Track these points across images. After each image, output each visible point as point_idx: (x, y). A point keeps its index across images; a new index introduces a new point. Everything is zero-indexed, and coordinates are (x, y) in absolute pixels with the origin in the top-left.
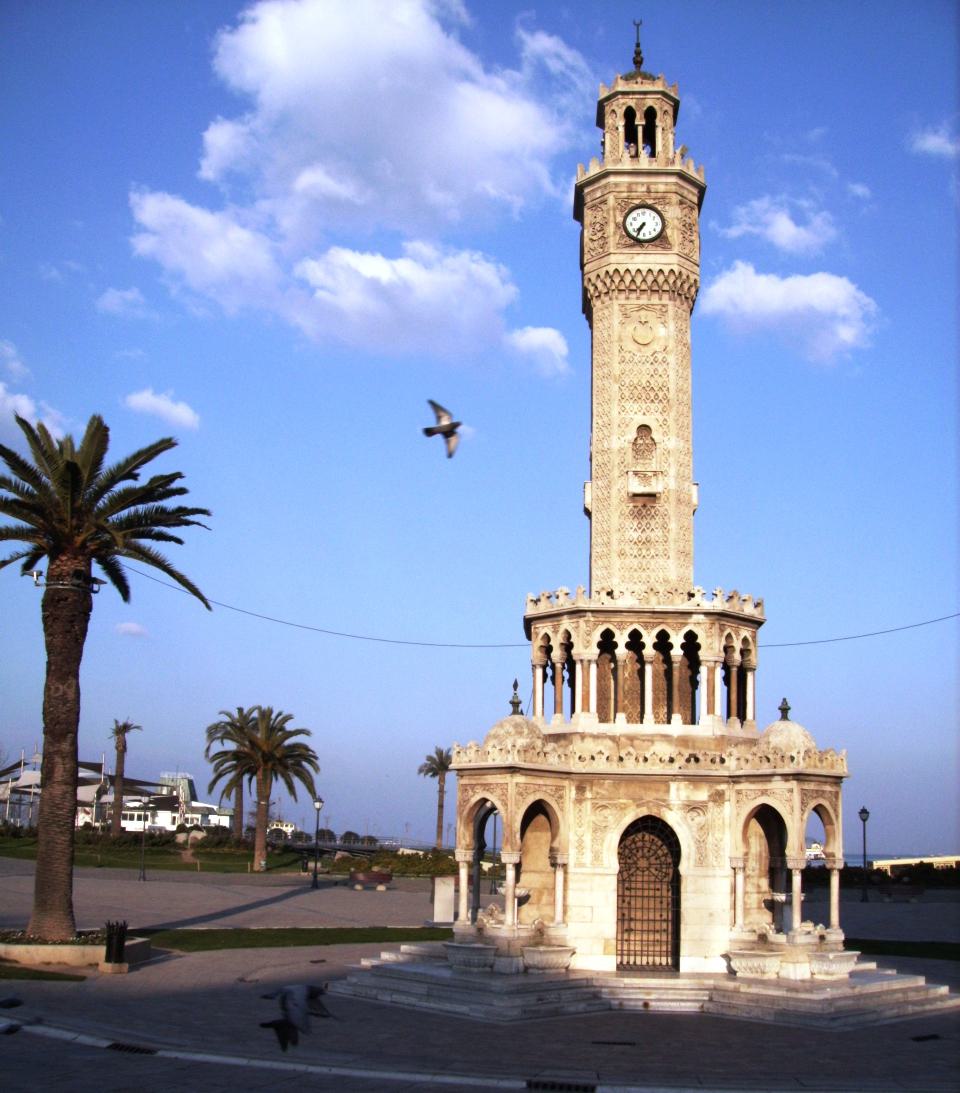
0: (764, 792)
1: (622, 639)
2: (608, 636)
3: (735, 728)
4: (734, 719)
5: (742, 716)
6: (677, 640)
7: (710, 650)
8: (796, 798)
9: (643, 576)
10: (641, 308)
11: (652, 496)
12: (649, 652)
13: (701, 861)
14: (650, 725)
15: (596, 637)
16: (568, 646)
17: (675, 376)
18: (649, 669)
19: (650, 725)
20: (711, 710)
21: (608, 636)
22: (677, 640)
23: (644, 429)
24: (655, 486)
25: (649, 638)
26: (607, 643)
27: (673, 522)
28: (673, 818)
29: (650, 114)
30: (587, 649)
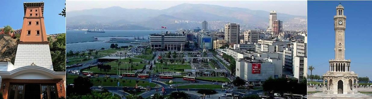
2: (337, 63)
5: (349, 71)
6: (343, 64)
7: (346, 64)
9: (340, 58)
11: (341, 50)
12: (340, 65)
13: (345, 84)
15: (336, 64)
16: (333, 64)
17: (343, 38)
21: (337, 63)
22: (343, 64)
23: (340, 43)
24: (341, 49)
26: (337, 64)
27: (343, 52)
28: (342, 80)
29: (341, 10)
30: (335, 65)
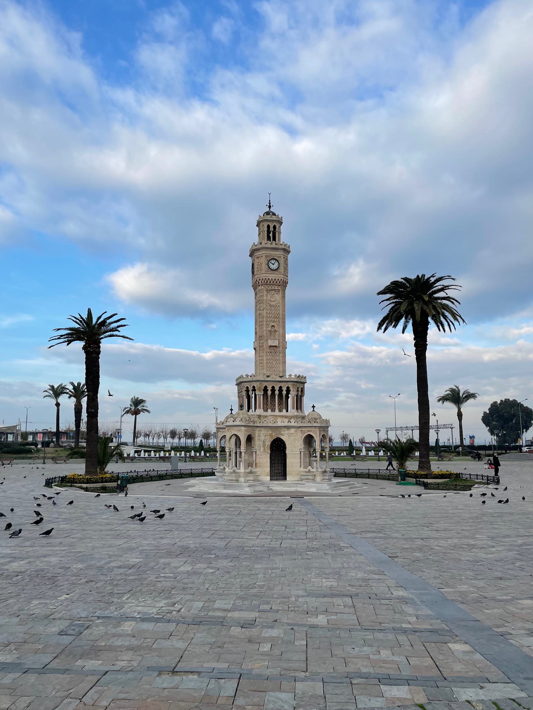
0: (309, 431)
1: (269, 388)
3: (300, 414)
4: (299, 410)
8: (318, 432)
10: (272, 290)
14: (277, 412)
18: (277, 397)
19: (277, 412)
20: (293, 408)
25: (277, 388)
